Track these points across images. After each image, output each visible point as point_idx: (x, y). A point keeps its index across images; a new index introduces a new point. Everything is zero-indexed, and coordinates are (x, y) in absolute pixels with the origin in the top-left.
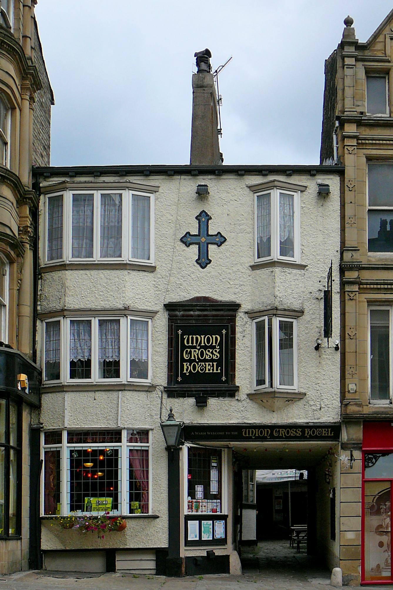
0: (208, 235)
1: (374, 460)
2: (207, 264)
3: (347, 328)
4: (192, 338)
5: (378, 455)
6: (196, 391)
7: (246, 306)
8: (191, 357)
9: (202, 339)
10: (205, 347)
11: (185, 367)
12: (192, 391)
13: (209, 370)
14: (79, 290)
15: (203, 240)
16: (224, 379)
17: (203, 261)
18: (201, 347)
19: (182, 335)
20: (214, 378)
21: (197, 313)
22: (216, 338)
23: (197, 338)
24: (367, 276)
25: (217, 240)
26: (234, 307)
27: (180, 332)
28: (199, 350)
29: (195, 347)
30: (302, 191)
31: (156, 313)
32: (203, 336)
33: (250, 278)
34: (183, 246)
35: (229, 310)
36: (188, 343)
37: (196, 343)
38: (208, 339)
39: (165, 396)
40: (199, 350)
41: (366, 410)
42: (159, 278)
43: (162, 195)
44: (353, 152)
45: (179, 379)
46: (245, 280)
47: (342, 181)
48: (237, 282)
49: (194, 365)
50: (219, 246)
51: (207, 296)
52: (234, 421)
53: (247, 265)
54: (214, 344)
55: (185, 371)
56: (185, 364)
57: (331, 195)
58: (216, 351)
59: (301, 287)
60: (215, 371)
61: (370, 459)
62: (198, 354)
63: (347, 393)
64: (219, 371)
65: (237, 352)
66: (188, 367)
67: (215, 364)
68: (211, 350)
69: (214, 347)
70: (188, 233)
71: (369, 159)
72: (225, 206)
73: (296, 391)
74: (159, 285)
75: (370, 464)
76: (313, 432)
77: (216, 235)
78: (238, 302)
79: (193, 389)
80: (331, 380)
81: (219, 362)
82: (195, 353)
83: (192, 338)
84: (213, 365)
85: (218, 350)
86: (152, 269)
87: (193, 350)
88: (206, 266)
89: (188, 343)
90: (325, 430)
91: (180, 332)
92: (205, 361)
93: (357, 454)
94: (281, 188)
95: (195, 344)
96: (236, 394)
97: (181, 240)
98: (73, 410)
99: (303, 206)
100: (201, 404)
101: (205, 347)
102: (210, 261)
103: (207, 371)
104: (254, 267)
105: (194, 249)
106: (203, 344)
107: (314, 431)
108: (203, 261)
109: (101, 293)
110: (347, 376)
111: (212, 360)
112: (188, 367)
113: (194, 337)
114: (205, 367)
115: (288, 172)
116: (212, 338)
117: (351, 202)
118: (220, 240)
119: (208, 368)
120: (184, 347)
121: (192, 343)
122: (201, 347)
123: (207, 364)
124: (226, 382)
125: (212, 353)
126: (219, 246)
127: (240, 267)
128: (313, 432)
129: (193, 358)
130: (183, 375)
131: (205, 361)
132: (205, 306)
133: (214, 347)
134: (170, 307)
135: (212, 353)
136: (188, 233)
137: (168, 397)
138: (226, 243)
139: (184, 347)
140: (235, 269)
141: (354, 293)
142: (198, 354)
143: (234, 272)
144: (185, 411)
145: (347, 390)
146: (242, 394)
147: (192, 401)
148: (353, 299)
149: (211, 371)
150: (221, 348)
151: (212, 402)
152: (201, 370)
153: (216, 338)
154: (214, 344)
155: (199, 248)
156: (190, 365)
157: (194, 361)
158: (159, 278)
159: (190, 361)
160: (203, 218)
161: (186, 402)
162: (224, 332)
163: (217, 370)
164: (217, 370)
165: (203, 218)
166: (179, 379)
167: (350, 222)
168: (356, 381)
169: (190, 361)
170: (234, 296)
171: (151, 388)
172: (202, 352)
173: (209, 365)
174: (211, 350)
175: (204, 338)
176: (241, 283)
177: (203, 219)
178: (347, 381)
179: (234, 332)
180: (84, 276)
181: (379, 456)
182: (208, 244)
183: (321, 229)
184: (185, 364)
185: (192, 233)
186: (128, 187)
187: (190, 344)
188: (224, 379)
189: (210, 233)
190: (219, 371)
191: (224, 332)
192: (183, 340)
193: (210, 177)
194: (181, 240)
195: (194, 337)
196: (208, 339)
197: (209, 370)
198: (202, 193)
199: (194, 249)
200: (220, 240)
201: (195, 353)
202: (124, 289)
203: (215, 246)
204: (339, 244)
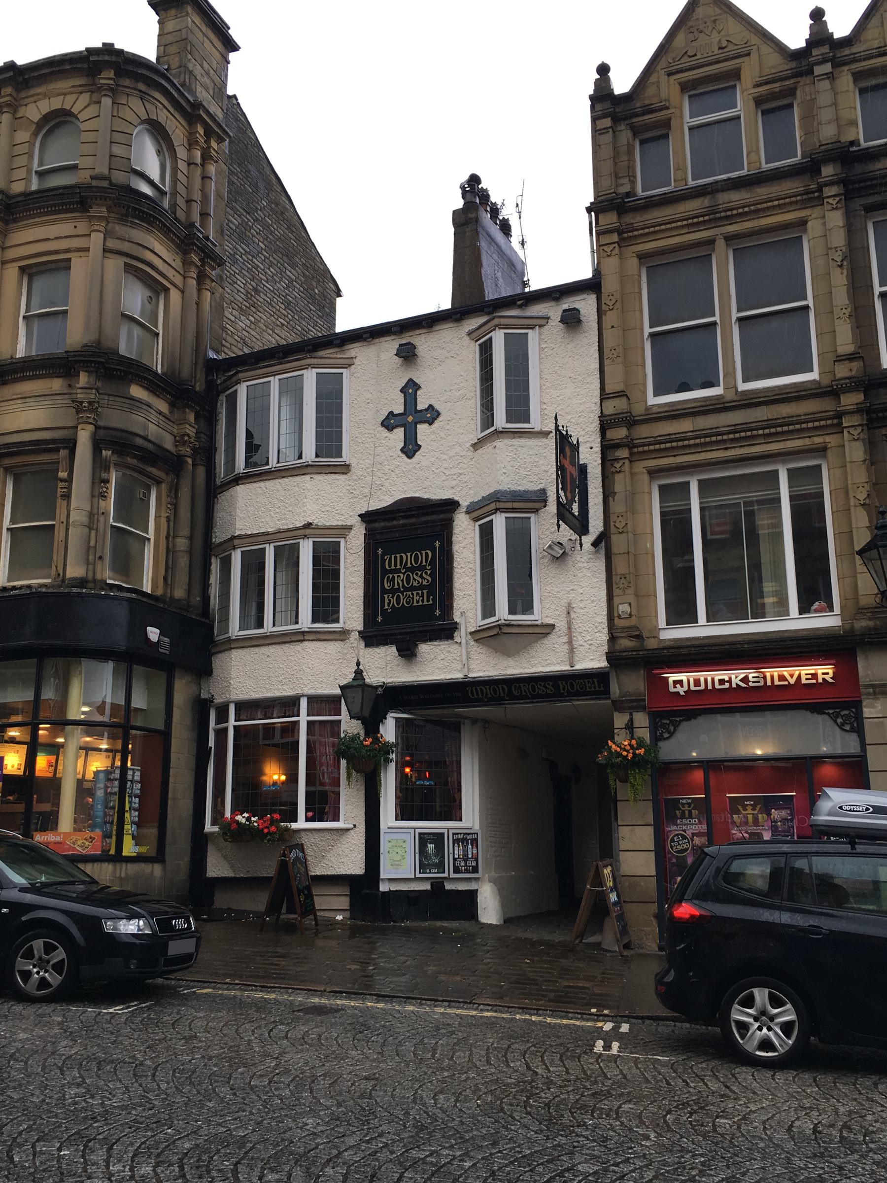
0: (417, 411)
1: (672, 728)
2: (416, 451)
3: (613, 518)
4: (396, 557)
5: (678, 719)
6: (400, 634)
7: (464, 503)
8: (394, 585)
9: (408, 558)
10: (413, 569)
11: (387, 601)
12: (395, 634)
13: (418, 602)
14: (253, 510)
15: (410, 419)
16: (438, 613)
17: (411, 448)
18: (408, 569)
19: (383, 555)
20: (425, 612)
21: (402, 522)
22: (426, 553)
23: (401, 557)
24: (645, 432)
25: (429, 415)
26: (451, 505)
27: (380, 551)
28: (404, 574)
29: (397, 571)
30: (540, 326)
31: (350, 528)
32: (409, 554)
33: (472, 463)
34: (385, 433)
35: (443, 512)
36: (390, 566)
37: (401, 565)
38: (416, 556)
39: (362, 644)
40: (404, 574)
41: (651, 644)
42: (356, 480)
43: (359, 367)
44: (613, 253)
45: (380, 619)
46: (465, 466)
47: (599, 299)
48: (454, 471)
49: (398, 596)
50: (430, 424)
51: (417, 495)
52: (455, 674)
53: (468, 445)
54: (424, 563)
55: (386, 607)
56: (386, 596)
57: (585, 325)
58: (426, 573)
59: (543, 464)
60: (426, 603)
61: (664, 726)
62: (402, 581)
63: (616, 620)
64: (431, 602)
65: (456, 570)
66: (390, 600)
67: (425, 592)
68: (419, 573)
69: (422, 568)
70: (391, 413)
71: (642, 257)
72: (440, 368)
73: (539, 623)
74: (355, 490)
75: (666, 735)
76: (572, 686)
77: (427, 410)
78: (456, 498)
79: (396, 632)
80: (593, 601)
81: (431, 588)
82: (399, 580)
83: (396, 557)
84: (423, 593)
85: (429, 572)
86: (345, 469)
87: (396, 575)
88: (414, 454)
89: (390, 566)
90: (589, 682)
91: (380, 551)
92: (413, 588)
93: (641, 720)
94: (506, 327)
95: (398, 567)
96: (456, 634)
97: (383, 424)
98: (247, 675)
99: (543, 346)
100: (408, 653)
101: (413, 569)
102: (420, 447)
103: (415, 604)
104: (476, 446)
105: (399, 432)
106: (409, 565)
107: (571, 683)
108: (411, 448)
109: (277, 510)
110: (616, 592)
111: (421, 587)
112: (390, 600)
113: (398, 556)
114: (413, 598)
115: (519, 303)
116: (421, 554)
117: (613, 327)
118: (431, 415)
119: (416, 599)
120: (385, 572)
121: (396, 565)
122: (408, 569)
123: (415, 593)
124: (442, 617)
125: (421, 576)
126: (430, 424)
127: (458, 449)
128: (572, 686)
129: (396, 586)
130: (384, 611)
131: (413, 588)
132: (410, 509)
133: (422, 568)
134: (367, 517)
135: (421, 576)
136: (391, 413)
137: (366, 646)
138: (440, 419)
139: (385, 572)
140: (452, 453)
141: (621, 462)
142: (402, 581)
143: (450, 458)
144: (384, 667)
145: (616, 615)
146: (462, 635)
147: (392, 650)
148: (620, 472)
149: (420, 603)
150: (433, 569)
151: (424, 648)
152: (407, 603)
153: (426, 553)
154: (424, 563)
155: (405, 430)
156: (393, 597)
157: (398, 590)
158: (356, 480)
159: (393, 591)
160: (411, 389)
161: (388, 652)
162: (437, 544)
163: (428, 601)
164: (428, 601)
165: (411, 389)
166: (380, 619)
167: (611, 356)
168: (632, 599)
169: (393, 591)
170: (451, 491)
171: (343, 635)
172: (408, 576)
173: (418, 594)
174: (419, 573)
175: (411, 555)
176: (461, 471)
177: (410, 391)
178: (616, 600)
179: (450, 543)
180: (259, 491)
181: (680, 721)
182: (416, 424)
183: (570, 375)
184: (386, 596)
185: (396, 412)
186: (309, 365)
187: (393, 567)
188: (438, 613)
189: (419, 408)
190: (431, 602)
191: (437, 544)
192: (384, 561)
193: (417, 332)
194: (383, 424)
195: (398, 556)
196: (416, 556)
197: (418, 602)
198: (408, 354)
199: (399, 432)
200: (431, 415)
201: (399, 580)
202: (305, 500)
203: (426, 426)
204: (597, 392)
